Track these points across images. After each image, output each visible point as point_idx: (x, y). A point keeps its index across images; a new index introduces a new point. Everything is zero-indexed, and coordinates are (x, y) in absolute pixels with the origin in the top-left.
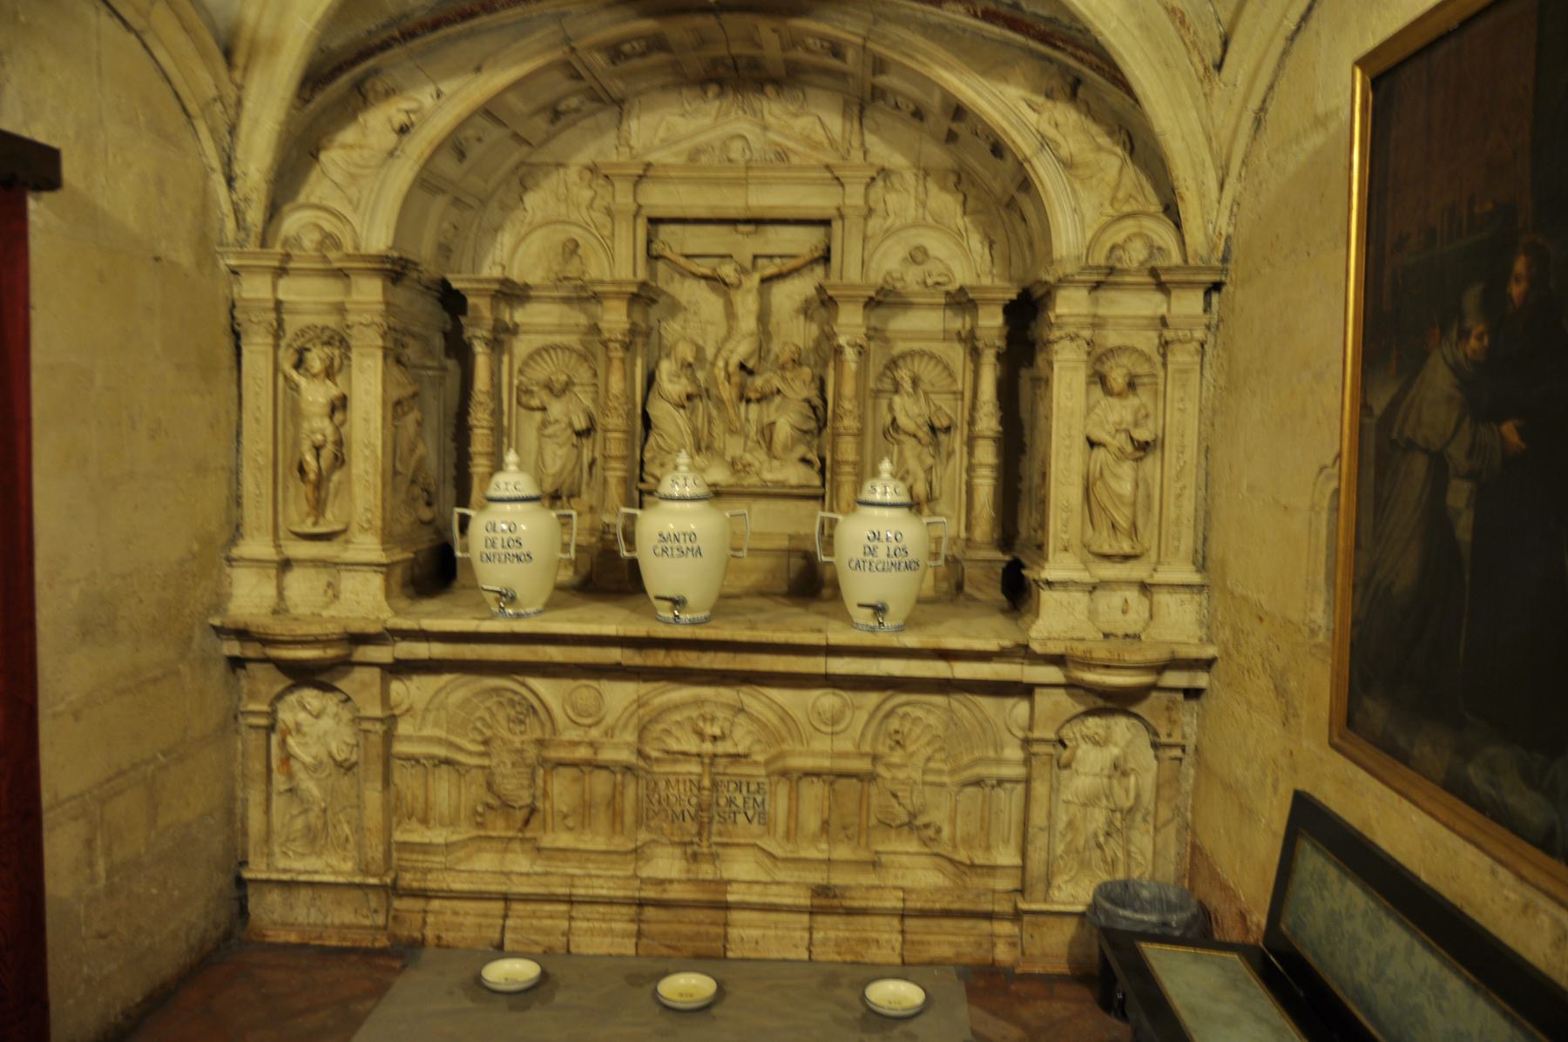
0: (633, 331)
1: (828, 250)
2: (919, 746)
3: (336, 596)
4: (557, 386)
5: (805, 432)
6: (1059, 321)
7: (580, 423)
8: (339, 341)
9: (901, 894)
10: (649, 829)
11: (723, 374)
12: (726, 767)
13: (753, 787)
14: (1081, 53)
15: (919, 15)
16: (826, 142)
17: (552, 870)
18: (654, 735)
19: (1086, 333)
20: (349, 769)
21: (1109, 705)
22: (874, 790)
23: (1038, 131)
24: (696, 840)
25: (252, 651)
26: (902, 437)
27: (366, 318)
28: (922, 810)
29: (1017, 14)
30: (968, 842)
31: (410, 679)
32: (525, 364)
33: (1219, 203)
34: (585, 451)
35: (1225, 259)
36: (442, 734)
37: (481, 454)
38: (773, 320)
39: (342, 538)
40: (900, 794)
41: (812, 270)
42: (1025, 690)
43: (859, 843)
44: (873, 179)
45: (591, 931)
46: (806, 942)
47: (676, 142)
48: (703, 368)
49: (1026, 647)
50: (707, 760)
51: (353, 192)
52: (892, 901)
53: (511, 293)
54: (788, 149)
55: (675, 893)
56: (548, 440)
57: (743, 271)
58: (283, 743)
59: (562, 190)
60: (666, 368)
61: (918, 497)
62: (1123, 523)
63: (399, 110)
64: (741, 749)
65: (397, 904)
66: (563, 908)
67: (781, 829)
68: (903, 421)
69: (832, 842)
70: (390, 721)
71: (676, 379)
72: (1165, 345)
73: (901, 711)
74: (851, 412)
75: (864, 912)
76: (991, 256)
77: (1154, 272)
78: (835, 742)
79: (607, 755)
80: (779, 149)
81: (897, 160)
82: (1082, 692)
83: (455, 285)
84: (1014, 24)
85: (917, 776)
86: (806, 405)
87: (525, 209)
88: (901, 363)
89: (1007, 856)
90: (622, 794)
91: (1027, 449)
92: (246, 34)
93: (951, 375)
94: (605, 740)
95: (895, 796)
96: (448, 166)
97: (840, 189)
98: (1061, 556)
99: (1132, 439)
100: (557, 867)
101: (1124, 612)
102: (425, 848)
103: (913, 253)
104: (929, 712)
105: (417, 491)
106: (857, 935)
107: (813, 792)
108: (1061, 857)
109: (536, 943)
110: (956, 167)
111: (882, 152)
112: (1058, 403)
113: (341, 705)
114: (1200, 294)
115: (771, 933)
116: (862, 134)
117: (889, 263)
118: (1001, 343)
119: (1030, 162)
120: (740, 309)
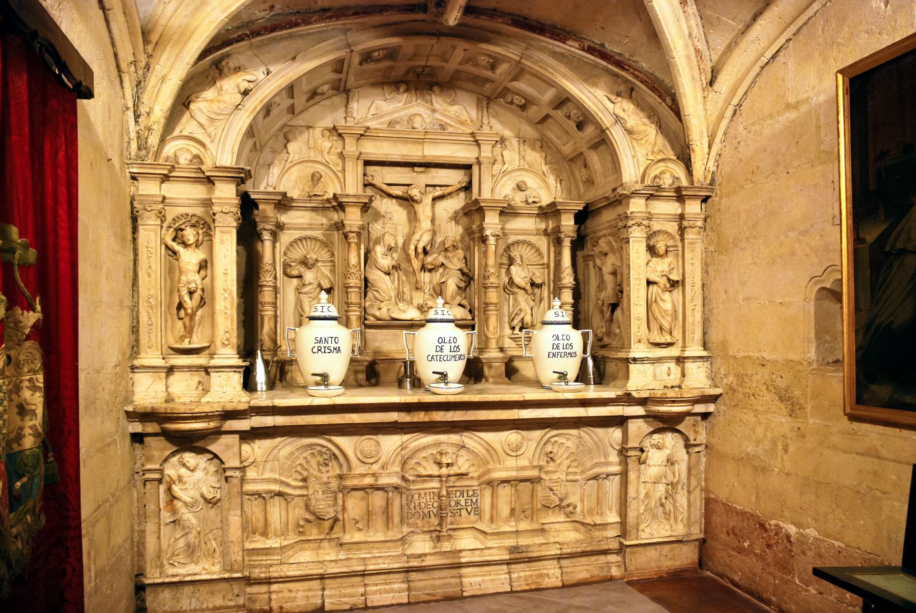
0: (362, 228)
2: (563, 460)
4: (311, 262)
6: (632, 215)
8: (206, 225)
10: (409, 525)
13: (471, 493)
14: (637, 73)
15: (550, 46)
18: (411, 467)
19: (645, 222)
20: (215, 504)
21: (665, 426)
22: (539, 488)
24: (438, 528)
25: (152, 428)
26: (516, 290)
27: (226, 209)
29: (605, 50)
31: (254, 442)
32: (288, 249)
33: (709, 154)
35: (711, 184)
36: (276, 476)
37: (269, 303)
38: (437, 223)
39: (207, 352)
41: (458, 194)
42: (621, 421)
43: (532, 519)
47: (381, 117)
49: (629, 394)
50: (444, 479)
51: (210, 129)
53: (284, 203)
54: (446, 123)
58: (169, 490)
60: (379, 250)
61: (527, 324)
62: (666, 325)
64: (463, 470)
67: (487, 516)
68: (518, 280)
69: (518, 520)
70: (243, 469)
72: (682, 230)
73: (553, 440)
77: (678, 190)
79: (383, 481)
81: (507, 133)
82: (651, 419)
83: (253, 197)
84: (604, 55)
85: (563, 477)
86: (459, 272)
87: (288, 153)
88: (512, 248)
90: (392, 504)
91: (582, 296)
92: (163, 21)
93: (540, 254)
94: (382, 471)
95: (551, 490)
99: (669, 280)
101: (669, 375)
102: (267, 551)
104: (569, 439)
107: (505, 492)
110: (539, 138)
111: (498, 127)
113: (208, 462)
114: (699, 202)
117: (505, 190)
118: (574, 235)
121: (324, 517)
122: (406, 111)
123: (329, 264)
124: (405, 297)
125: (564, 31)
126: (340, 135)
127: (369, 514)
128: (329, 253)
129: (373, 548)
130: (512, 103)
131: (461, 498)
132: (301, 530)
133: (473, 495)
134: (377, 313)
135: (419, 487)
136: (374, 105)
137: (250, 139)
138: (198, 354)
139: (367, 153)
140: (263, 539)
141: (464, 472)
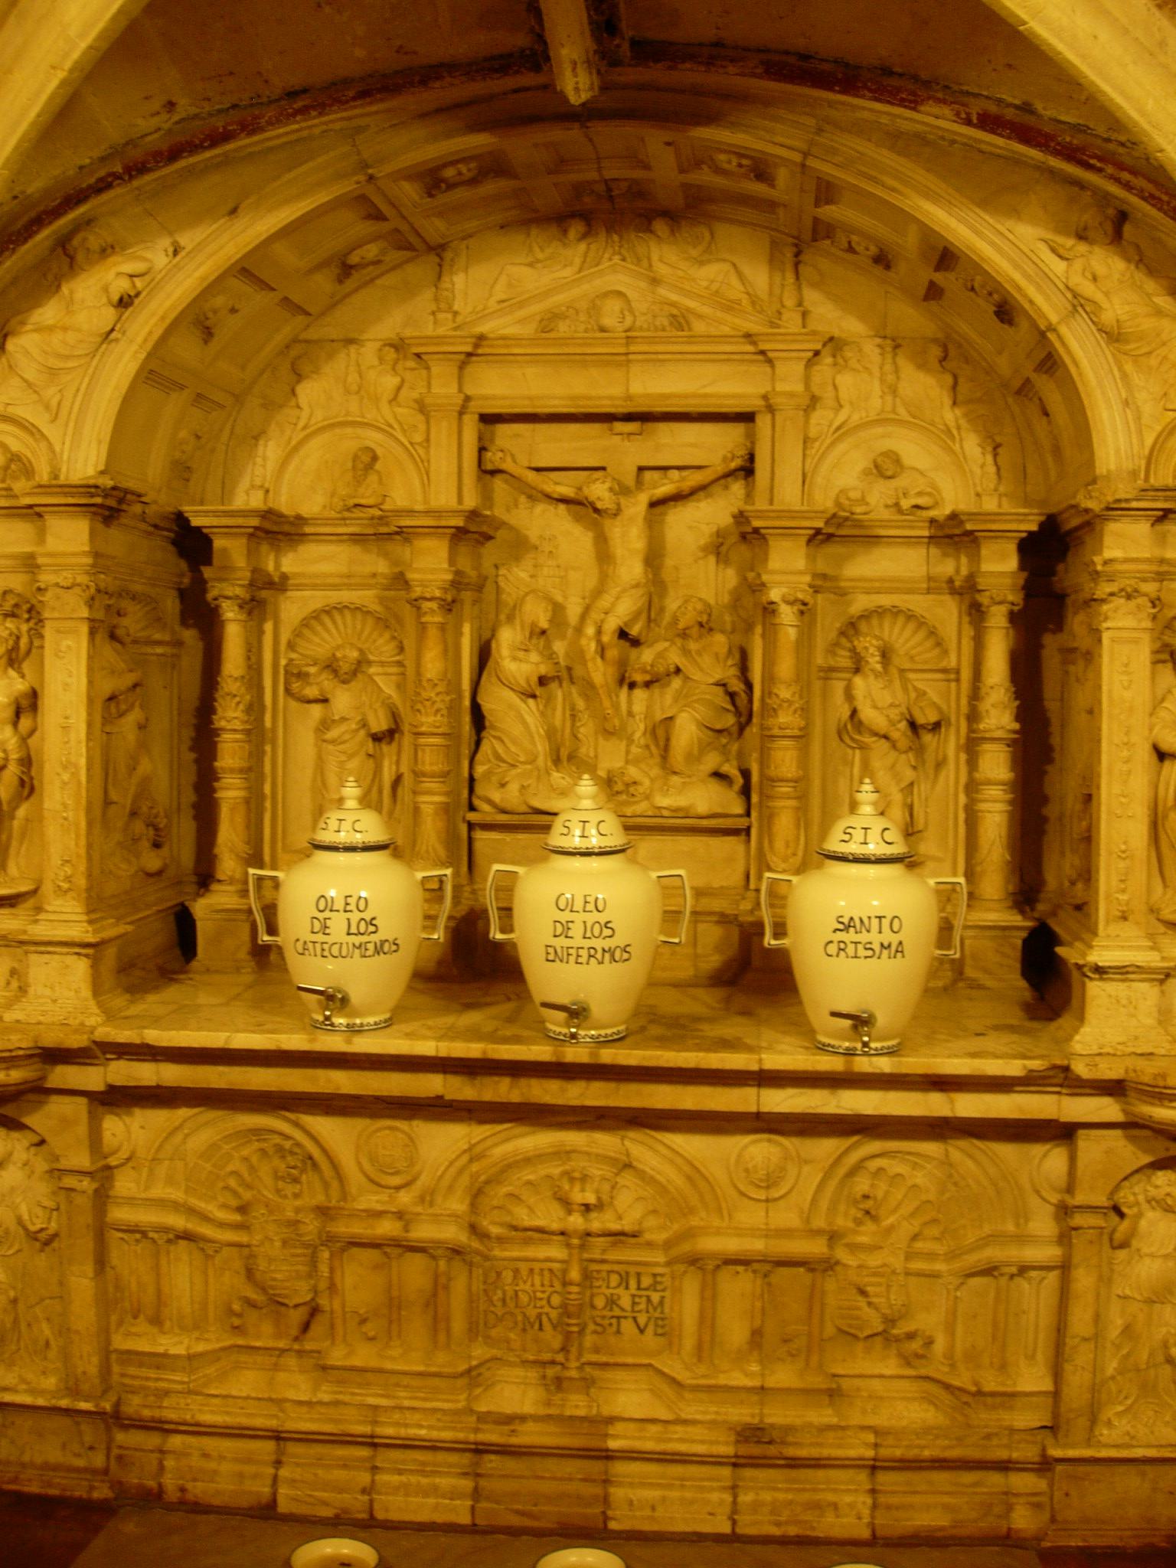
0: (458, 583)
1: (752, 457)
3: (23, 990)
4: (345, 667)
5: (720, 731)
6: (1108, 568)
7: (380, 723)
9: (871, 1438)
10: (489, 1341)
11: (593, 645)
12: (604, 1251)
13: (646, 1281)
14: (1125, 176)
15: (884, 120)
16: (745, 302)
17: (346, 1398)
18: (495, 1203)
19: (1150, 588)
20: (47, 1243)
22: (830, 1285)
23: (1068, 287)
24: (560, 1358)
26: (868, 739)
27: (65, 578)
28: (905, 1313)
30: (972, 1357)
31: (130, 1114)
32: (298, 634)
34: (386, 763)
36: (177, 1195)
37: (232, 771)
38: (669, 562)
39: (31, 903)
40: (869, 1289)
41: (726, 487)
42: (1064, 1132)
44: (817, 353)
45: (405, 1489)
46: (727, 1510)
47: (521, 305)
48: (563, 637)
49: (1066, 1069)
50: (575, 1241)
51: (51, 393)
52: (859, 1448)
54: (688, 310)
55: (530, 1435)
56: (330, 747)
57: (622, 490)
59: (353, 377)
60: (507, 638)
63: (119, 274)
64: (626, 1225)
65: (120, 1437)
66: (364, 1452)
67: (689, 1343)
68: (867, 714)
70: (104, 1175)
71: (521, 654)
74: (790, 703)
75: (816, 1463)
76: (996, 463)
78: (771, 1214)
79: (423, 1232)
80: (675, 312)
81: (851, 326)
82: (1147, 1133)
83: (195, 522)
84: (1026, 134)
85: (897, 1263)
86: (720, 690)
87: (298, 407)
88: (863, 626)
89: (1033, 1379)
90: (446, 1288)
91: (1056, 755)
95: (863, 1292)
96: (188, 350)
97: (768, 369)
98: (1115, 929)
100: (353, 1394)
102: (160, 1361)
103: (879, 460)
105: (139, 826)
106: (806, 1496)
107: (737, 1287)
108: (1113, 1378)
109: (325, 1503)
110: (940, 335)
112: (1110, 691)
113: (33, 1150)
115: (675, 1494)
116: (799, 288)
118: (1016, 597)
119: (1055, 330)
120: (618, 550)
121: (286, 1301)
122: (586, 287)
123: (394, 670)
124: (583, 750)
125: (915, 78)
126: (418, 355)
127: (393, 1307)
128: (393, 644)
129: (397, 1385)
130: (851, 249)
131: (621, 1291)
132: (236, 1322)
133: (653, 1287)
134: (496, 796)
135: (515, 1254)
136: (503, 280)
137: (174, 395)
138: (12, 906)
139: (486, 398)
140: (155, 1330)
141: (627, 1228)
